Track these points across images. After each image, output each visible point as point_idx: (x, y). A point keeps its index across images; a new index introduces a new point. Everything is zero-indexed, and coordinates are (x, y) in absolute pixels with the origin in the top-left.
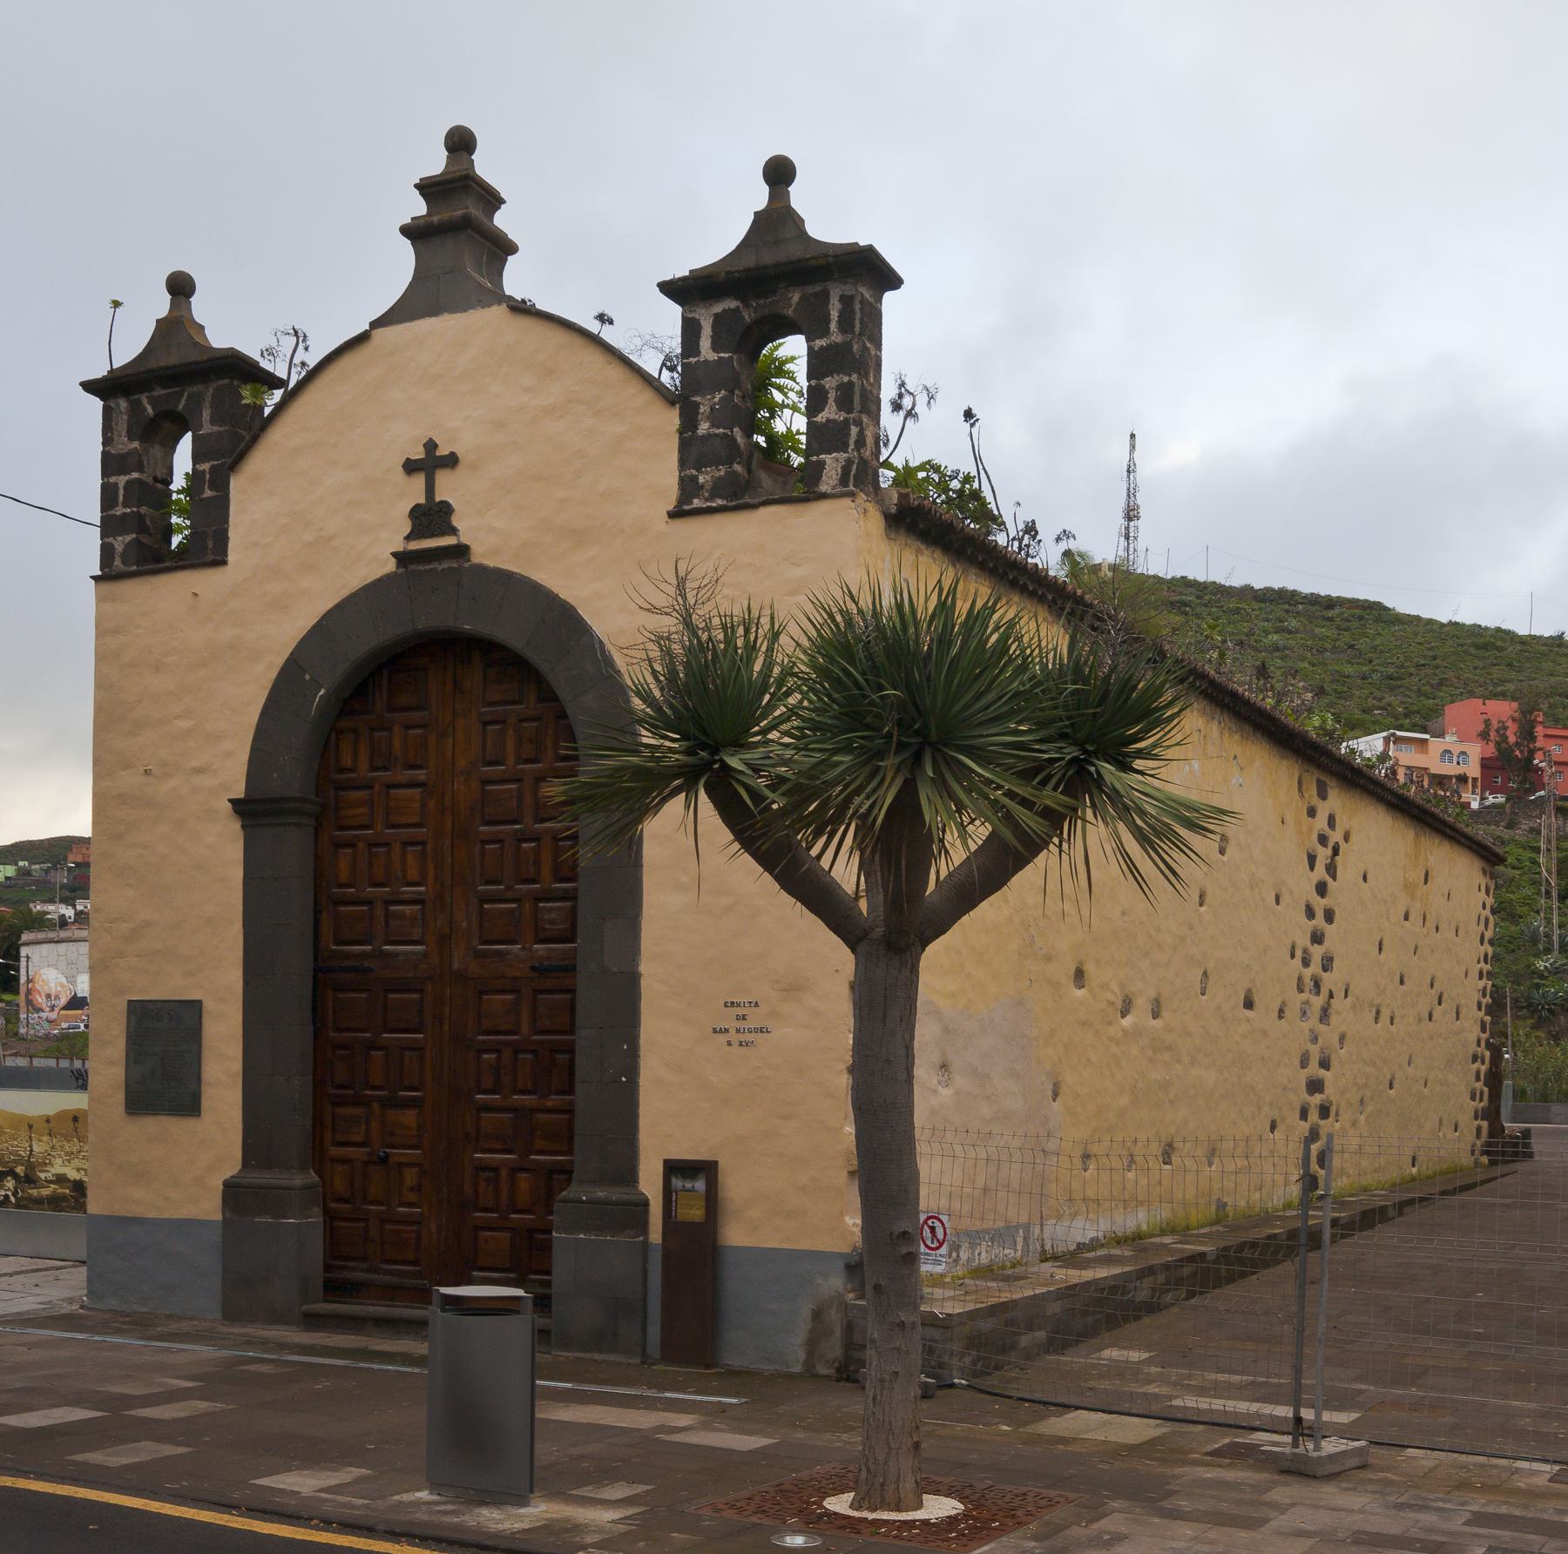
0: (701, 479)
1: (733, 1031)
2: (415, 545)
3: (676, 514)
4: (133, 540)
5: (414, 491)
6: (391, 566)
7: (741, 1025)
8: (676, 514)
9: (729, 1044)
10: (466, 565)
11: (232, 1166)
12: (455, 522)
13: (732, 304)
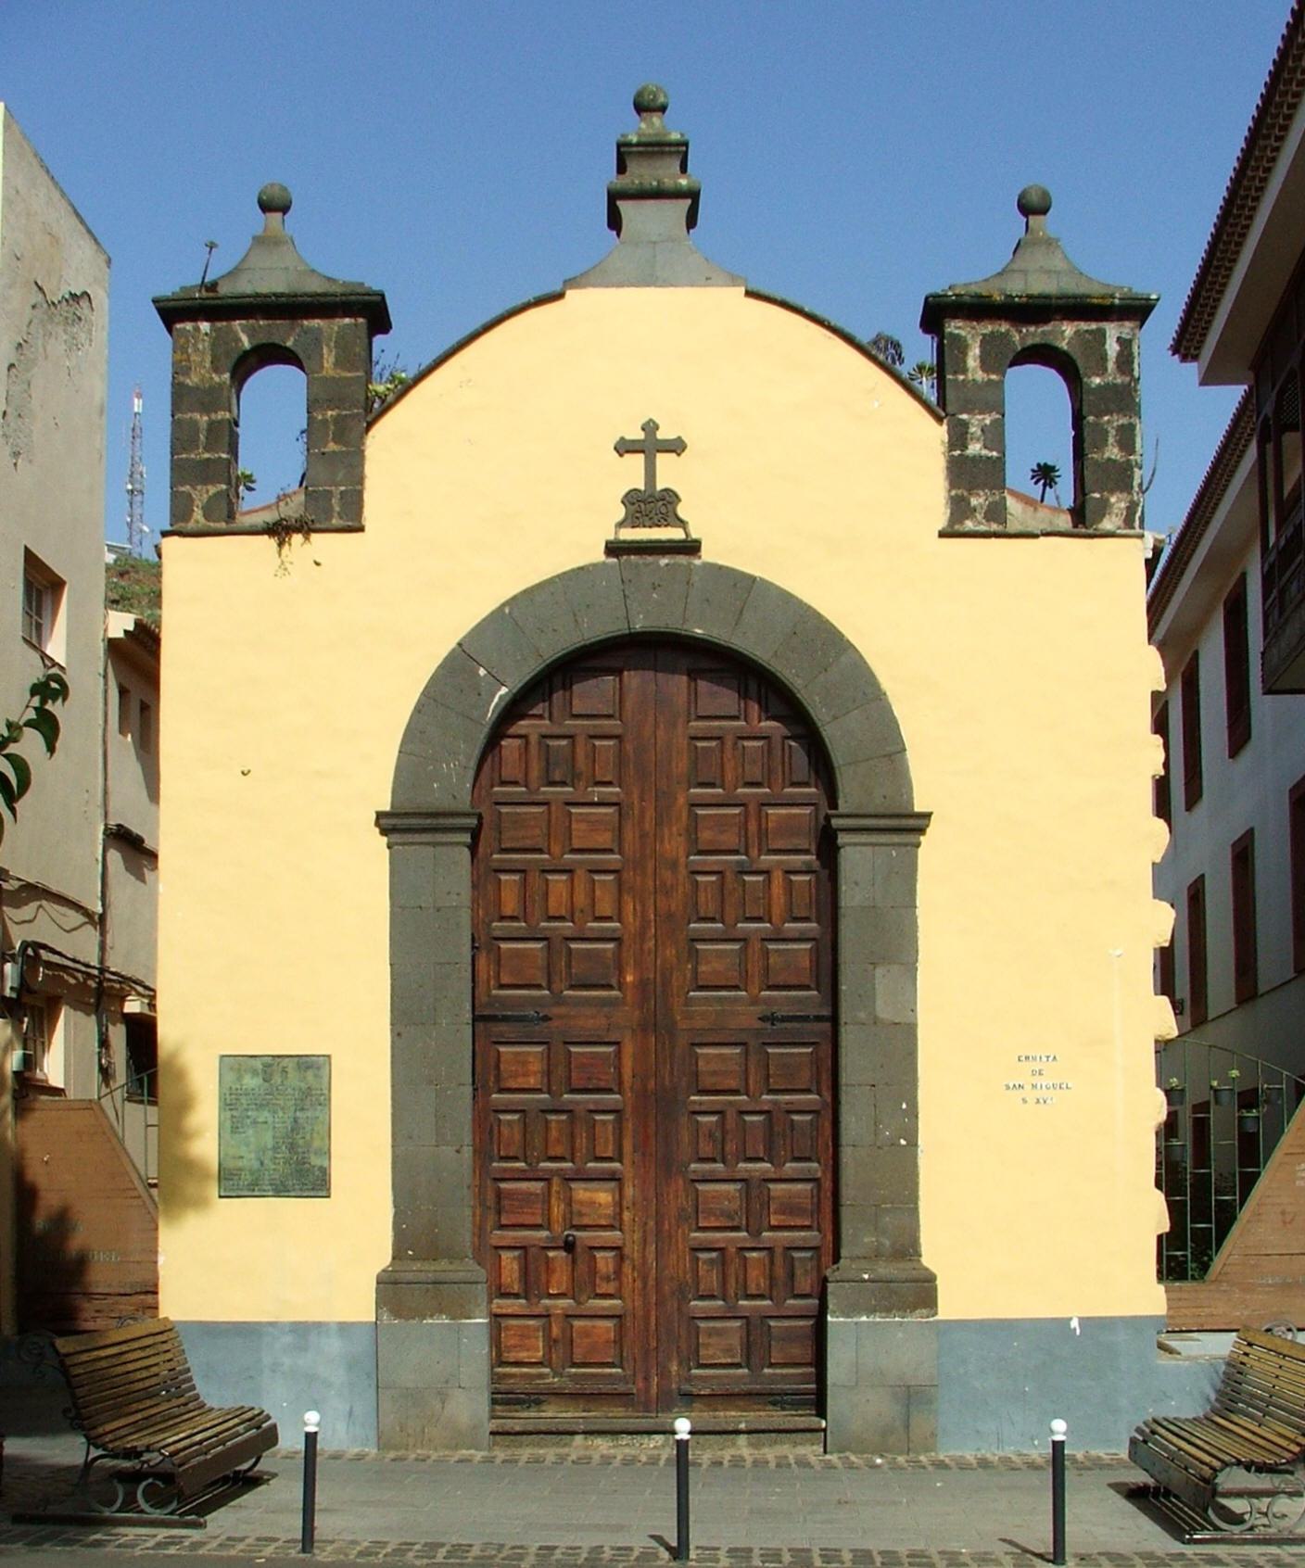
0: (974, 502)
1: (1027, 1087)
2: (629, 534)
3: (942, 535)
4: (219, 494)
5: (631, 473)
6: (598, 556)
7: (1037, 1080)
8: (942, 535)
9: (1025, 1101)
10: (697, 562)
11: (382, 1256)
12: (682, 511)
13: (1004, 327)
